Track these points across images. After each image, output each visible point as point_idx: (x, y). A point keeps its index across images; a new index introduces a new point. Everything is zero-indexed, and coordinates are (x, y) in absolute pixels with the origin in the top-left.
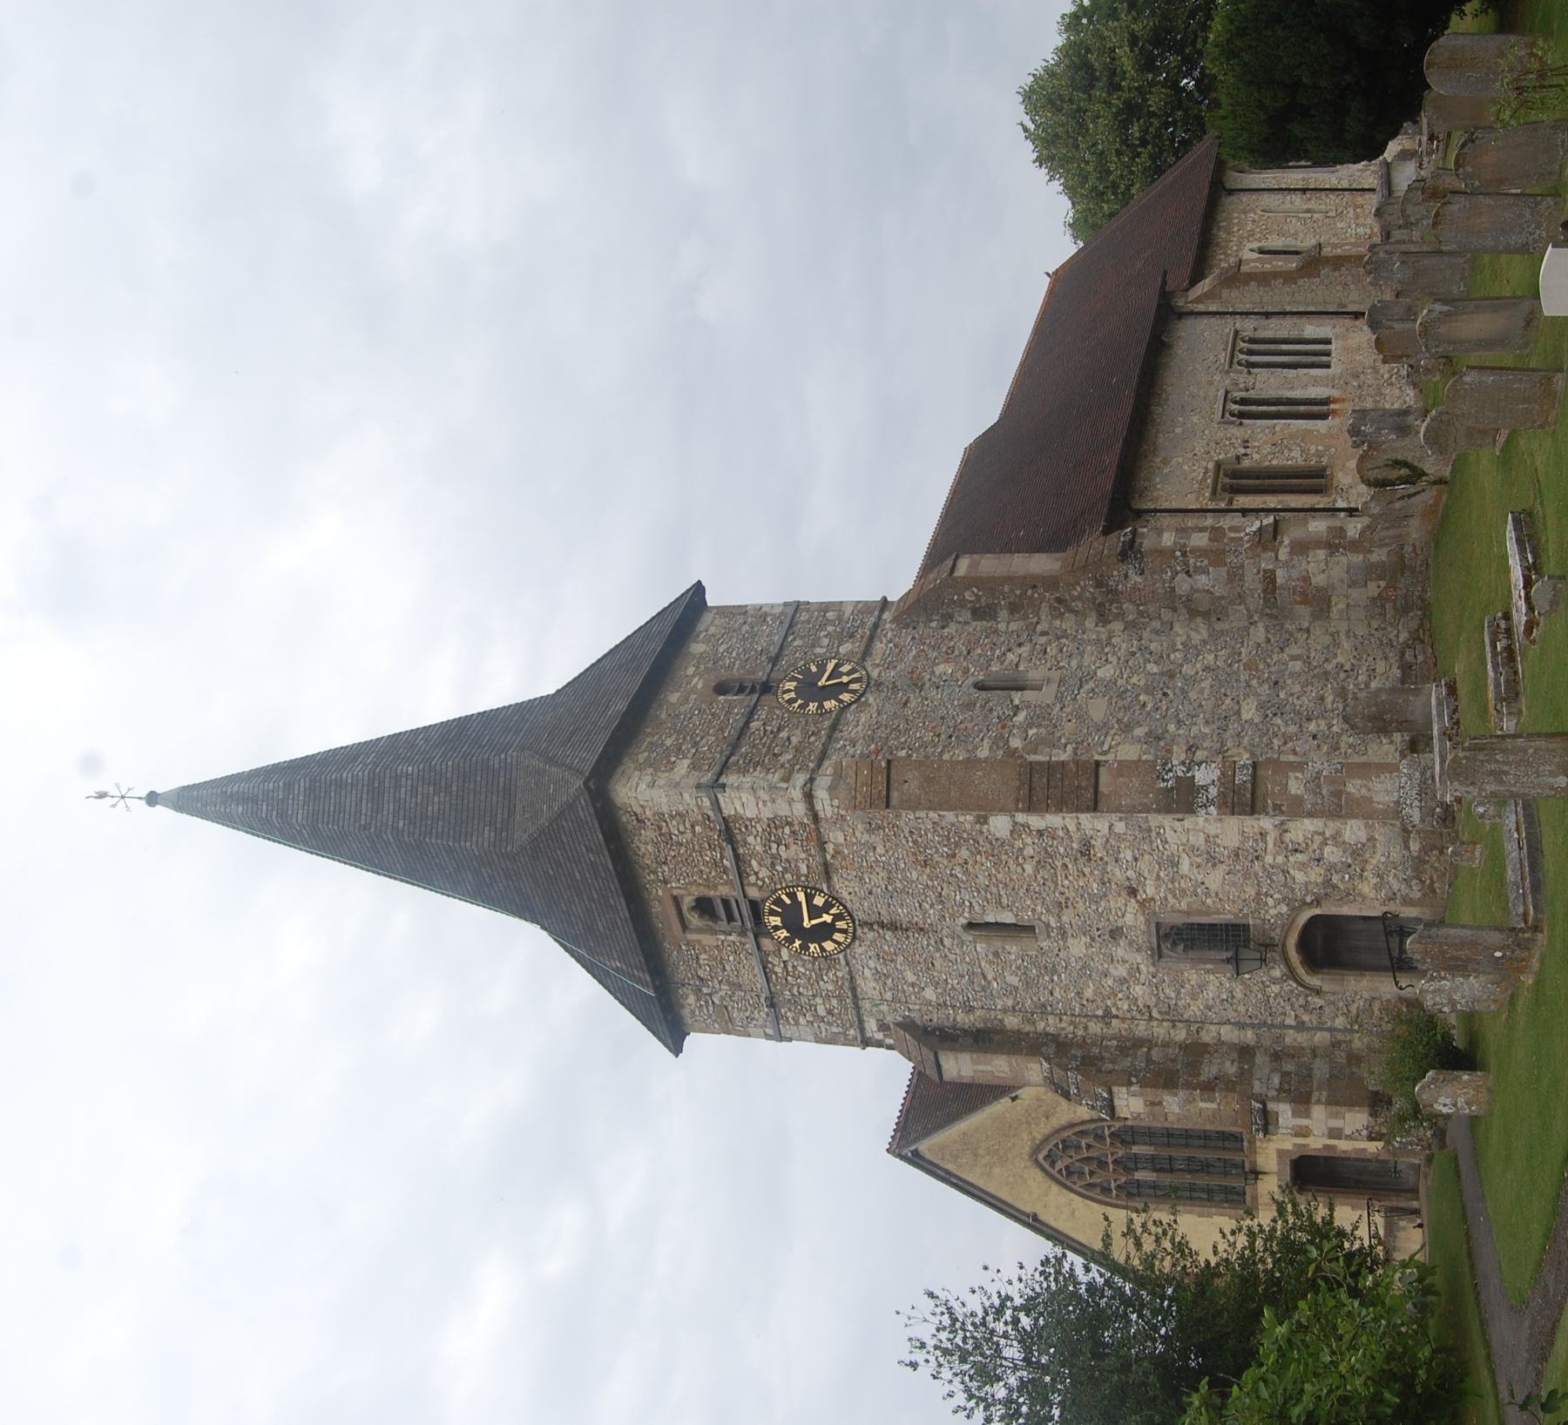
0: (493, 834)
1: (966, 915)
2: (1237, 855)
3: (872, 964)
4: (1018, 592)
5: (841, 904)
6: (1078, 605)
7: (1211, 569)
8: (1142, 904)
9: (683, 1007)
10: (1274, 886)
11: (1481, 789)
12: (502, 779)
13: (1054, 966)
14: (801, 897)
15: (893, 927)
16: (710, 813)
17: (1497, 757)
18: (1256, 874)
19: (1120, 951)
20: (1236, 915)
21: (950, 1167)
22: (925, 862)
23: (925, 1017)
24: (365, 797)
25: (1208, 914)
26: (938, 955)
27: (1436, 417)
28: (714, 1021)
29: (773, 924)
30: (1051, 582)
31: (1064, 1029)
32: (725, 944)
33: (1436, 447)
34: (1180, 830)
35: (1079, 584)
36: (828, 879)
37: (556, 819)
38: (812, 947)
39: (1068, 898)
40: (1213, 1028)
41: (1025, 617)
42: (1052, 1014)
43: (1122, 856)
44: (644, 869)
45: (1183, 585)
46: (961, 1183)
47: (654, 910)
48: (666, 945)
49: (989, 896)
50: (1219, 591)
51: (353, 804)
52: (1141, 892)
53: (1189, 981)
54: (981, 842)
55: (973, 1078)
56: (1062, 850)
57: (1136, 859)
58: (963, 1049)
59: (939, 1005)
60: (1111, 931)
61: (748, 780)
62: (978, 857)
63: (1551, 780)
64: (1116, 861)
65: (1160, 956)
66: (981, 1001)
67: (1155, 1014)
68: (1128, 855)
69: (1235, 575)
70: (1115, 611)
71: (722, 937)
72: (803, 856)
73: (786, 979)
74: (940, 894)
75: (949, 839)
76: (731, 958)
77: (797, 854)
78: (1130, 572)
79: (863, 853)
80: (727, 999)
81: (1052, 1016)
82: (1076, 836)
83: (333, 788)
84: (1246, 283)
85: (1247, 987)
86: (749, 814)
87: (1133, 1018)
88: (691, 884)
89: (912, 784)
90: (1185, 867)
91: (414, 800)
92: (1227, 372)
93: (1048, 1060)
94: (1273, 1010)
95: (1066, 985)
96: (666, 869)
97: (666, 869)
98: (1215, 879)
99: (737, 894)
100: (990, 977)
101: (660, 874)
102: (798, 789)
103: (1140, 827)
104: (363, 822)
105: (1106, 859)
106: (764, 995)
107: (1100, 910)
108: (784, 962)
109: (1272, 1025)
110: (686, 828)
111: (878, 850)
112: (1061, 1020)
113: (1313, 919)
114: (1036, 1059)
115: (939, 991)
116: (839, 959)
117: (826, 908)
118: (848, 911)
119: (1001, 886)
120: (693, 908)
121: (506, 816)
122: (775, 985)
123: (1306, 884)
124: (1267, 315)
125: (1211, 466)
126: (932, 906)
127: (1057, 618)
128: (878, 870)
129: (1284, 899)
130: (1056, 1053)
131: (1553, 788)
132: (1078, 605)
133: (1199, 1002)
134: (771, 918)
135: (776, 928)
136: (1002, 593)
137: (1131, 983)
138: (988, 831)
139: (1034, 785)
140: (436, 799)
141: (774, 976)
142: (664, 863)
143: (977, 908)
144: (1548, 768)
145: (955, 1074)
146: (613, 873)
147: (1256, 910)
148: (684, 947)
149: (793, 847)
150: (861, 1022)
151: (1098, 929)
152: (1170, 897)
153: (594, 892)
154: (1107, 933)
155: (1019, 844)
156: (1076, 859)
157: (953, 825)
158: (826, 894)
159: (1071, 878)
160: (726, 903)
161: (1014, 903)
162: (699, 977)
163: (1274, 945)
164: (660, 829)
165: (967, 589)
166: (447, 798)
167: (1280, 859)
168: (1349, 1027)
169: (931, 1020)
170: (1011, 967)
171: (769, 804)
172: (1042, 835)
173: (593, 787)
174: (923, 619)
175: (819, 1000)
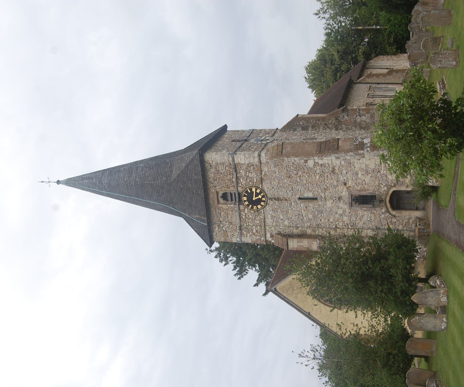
0: (165, 178)
1: (299, 194)
2: (374, 171)
3: (271, 213)
4: (314, 122)
5: (264, 192)
6: (330, 126)
7: (366, 114)
8: (347, 188)
9: (214, 232)
10: (383, 181)
11: (437, 66)
12: (169, 164)
13: (322, 211)
14: (254, 190)
15: (278, 199)
16: (231, 162)
17: (440, 56)
18: (379, 177)
19: (341, 205)
20: (373, 191)
21: (285, 295)
22: (289, 176)
23: (284, 231)
24: (127, 174)
25: (365, 191)
26: (290, 209)
27: (425, 40)
28: (222, 236)
29: (244, 199)
30: (324, 119)
31: (323, 233)
32: (229, 208)
33: (425, 49)
34: (359, 163)
35: (331, 119)
36: (262, 183)
37: (187, 166)
38: (255, 207)
39: (327, 187)
40: (365, 231)
41: (316, 130)
42: (321, 228)
43: (343, 172)
44: (210, 182)
45: (359, 119)
46: (288, 301)
47: (210, 197)
48: (212, 209)
49: (306, 187)
50: (368, 121)
51: (123, 176)
52: (348, 184)
53: (359, 214)
54: (305, 169)
55: (297, 248)
56: (327, 170)
57: (347, 173)
58: (295, 238)
59: (289, 226)
60: (339, 198)
61: (243, 153)
62: (304, 174)
63: (452, 63)
64: (341, 174)
65: (352, 206)
66: (301, 224)
67: (350, 227)
68: (344, 172)
69: (372, 116)
70: (340, 127)
71: (229, 206)
72: (255, 176)
73: (245, 220)
74: (292, 187)
75: (296, 168)
76: (230, 213)
77: (254, 175)
78: (345, 115)
79: (272, 174)
80: (227, 228)
81: (320, 229)
82: (331, 166)
83: (117, 172)
84: (373, 77)
85: (375, 216)
86: (242, 162)
87: (343, 228)
88: (222, 187)
89: (288, 149)
90: (360, 175)
91: (142, 173)
92: (368, 91)
93: (319, 240)
94: (382, 223)
95: (325, 217)
96: (216, 182)
97: (216, 182)
98: (368, 179)
99: (235, 190)
100: (304, 216)
101: (214, 184)
102: (257, 154)
103: (348, 162)
104: (125, 180)
105: (338, 173)
106: (238, 226)
107: (336, 191)
108: (246, 214)
109: (382, 229)
110: (224, 168)
111: (277, 173)
112: (323, 230)
113: (394, 192)
114: (316, 240)
115: (289, 221)
116: (261, 212)
117: (261, 193)
118: (266, 194)
119: (309, 183)
120: (222, 197)
121: (170, 173)
122: (242, 222)
123: (392, 180)
124: (379, 84)
125: (365, 103)
126: (290, 191)
127: (324, 130)
128: (276, 180)
129: (386, 185)
130: (321, 238)
131: (452, 65)
132: (330, 126)
133: (362, 222)
134: (244, 198)
135: (245, 201)
136: (310, 122)
137: (343, 216)
138: (307, 165)
139: (321, 147)
140: (149, 172)
141: (242, 219)
142: (216, 180)
143: (302, 191)
144: (451, 59)
145: (292, 247)
146: (202, 181)
147: (378, 189)
148: (217, 210)
149: (253, 173)
150: (265, 234)
151: (335, 197)
152: (355, 185)
153: (194, 190)
154: (338, 198)
155: (315, 169)
156: (331, 174)
157: (298, 163)
158: (260, 189)
159: (329, 180)
160: (231, 194)
161: (312, 189)
162: (220, 220)
163: (383, 201)
164: (216, 169)
165: (301, 121)
166: (152, 171)
167: (385, 172)
168: (403, 229)
169: (286, 232)
170: (310, 211)
171: (248, 159)
172: (322, 166)
173: (200, 152)
174: (288, 130)
175: (254, 227)
